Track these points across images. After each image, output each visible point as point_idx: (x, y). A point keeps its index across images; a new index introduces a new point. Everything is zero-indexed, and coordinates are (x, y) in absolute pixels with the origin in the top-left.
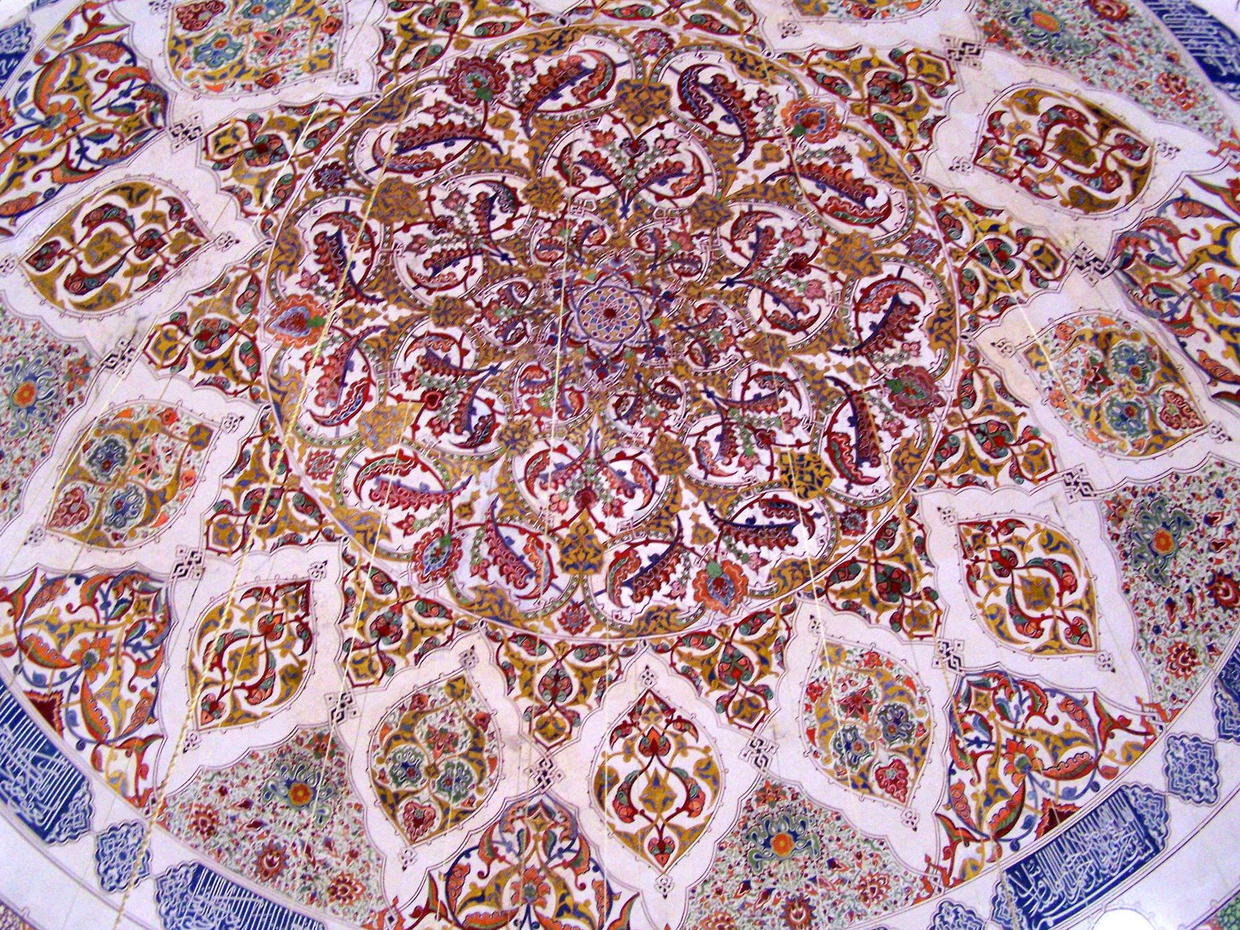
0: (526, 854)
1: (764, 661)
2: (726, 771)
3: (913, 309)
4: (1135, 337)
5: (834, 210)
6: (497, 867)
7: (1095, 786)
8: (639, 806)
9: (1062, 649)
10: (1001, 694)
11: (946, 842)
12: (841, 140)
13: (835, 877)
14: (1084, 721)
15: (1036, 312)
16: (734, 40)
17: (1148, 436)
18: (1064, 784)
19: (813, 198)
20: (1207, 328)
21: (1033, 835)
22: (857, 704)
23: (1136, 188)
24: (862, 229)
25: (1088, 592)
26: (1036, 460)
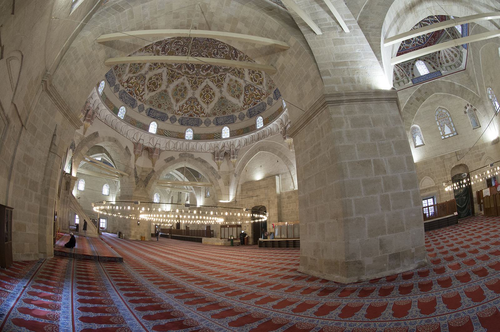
12: (176, 67)
16: (189, 76)
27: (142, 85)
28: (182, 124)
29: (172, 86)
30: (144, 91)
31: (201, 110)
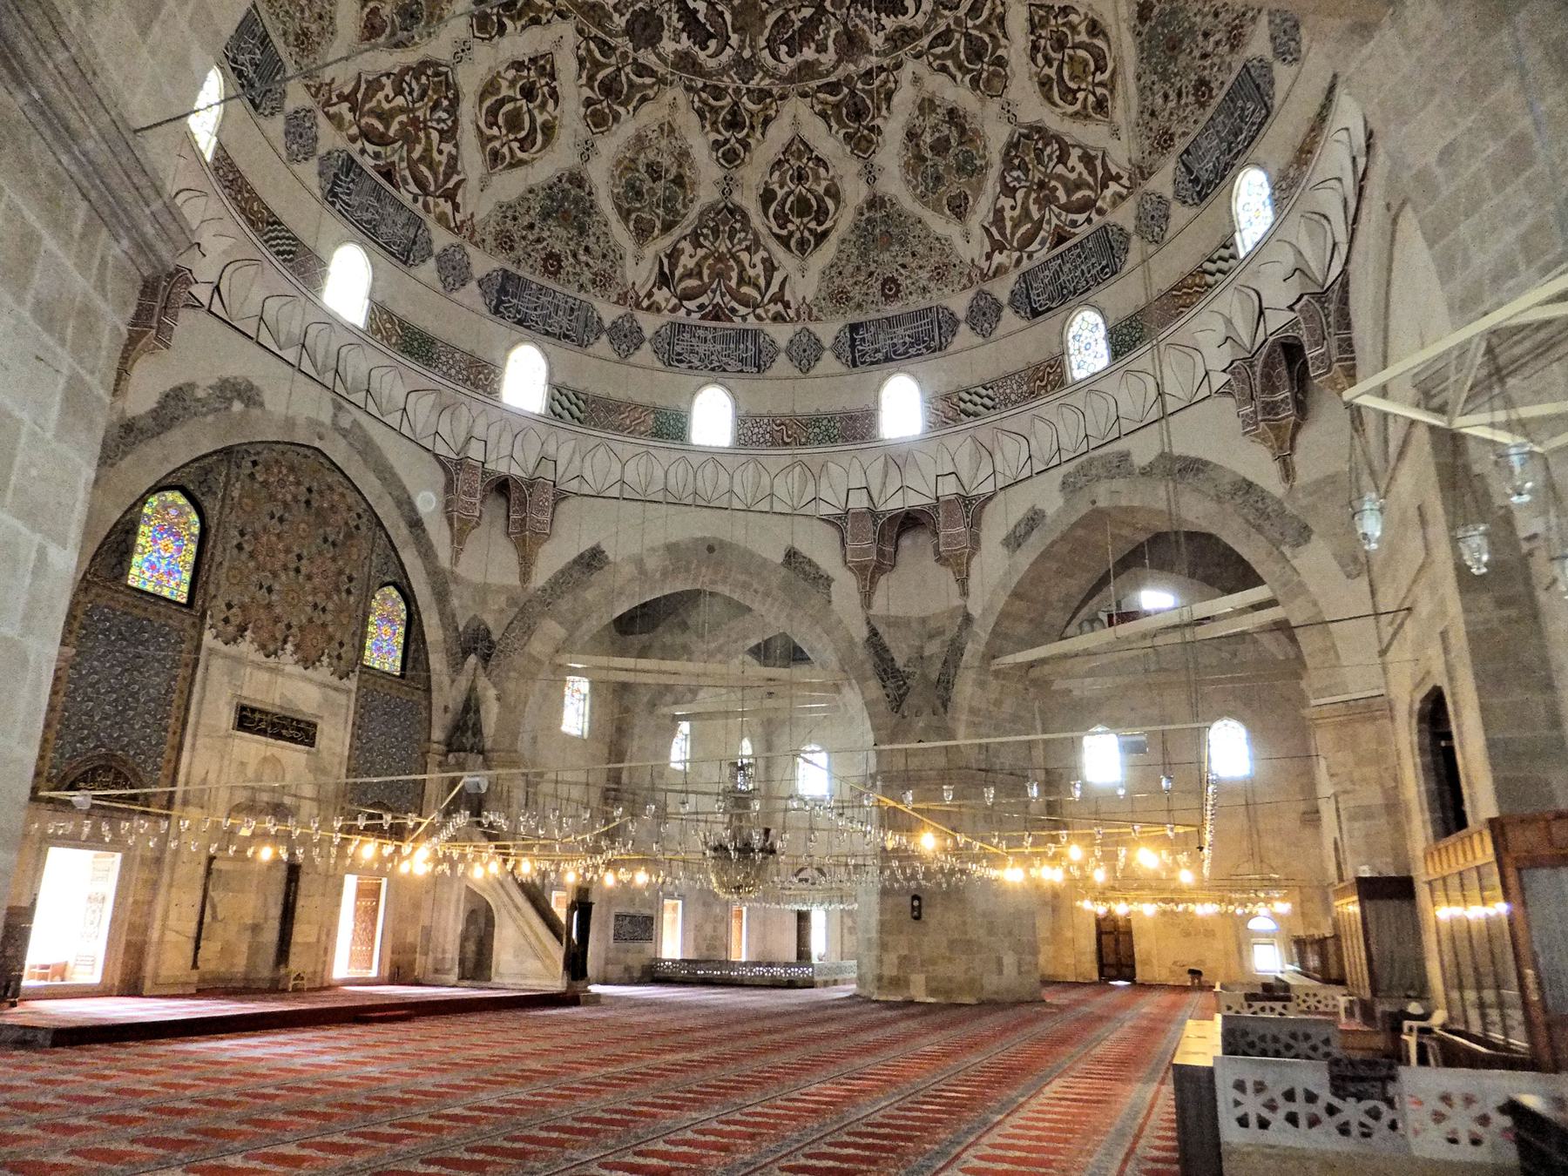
3: (704, 47)
4: (685, 206)
5: (783, 21)
9: (483, 147)
11: (347, 91)
15: (699, 143)
16: (925, 42)
17: (626, 206)
19: (798, 11)
23: (777, 237)
24: (766, 33)
25: (521, 163)
27: (748, 249)
28: (1036, 313)
29: (890, 154)
30: (774, 269)
31: (1093, 172)
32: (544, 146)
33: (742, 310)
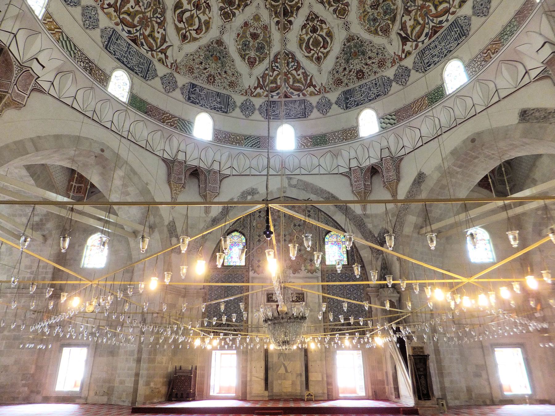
0: (146, 10)
1: (239, 6)
2: (212, 28)
4: (394, 4)
6: (137, 8)
7: (299, 96)
8: (184, 20)
9: (312, 60)
10: (290, 60)
11: (256, 85)
13: (224, 76)
14: (306, 80)
18: (292, 90)
20: (413, 17)
21: (278, 97)
22: (254, 36)
25: (328, 52)
26: (342, 12)
32: (331, 41)
33: (444, 18)
